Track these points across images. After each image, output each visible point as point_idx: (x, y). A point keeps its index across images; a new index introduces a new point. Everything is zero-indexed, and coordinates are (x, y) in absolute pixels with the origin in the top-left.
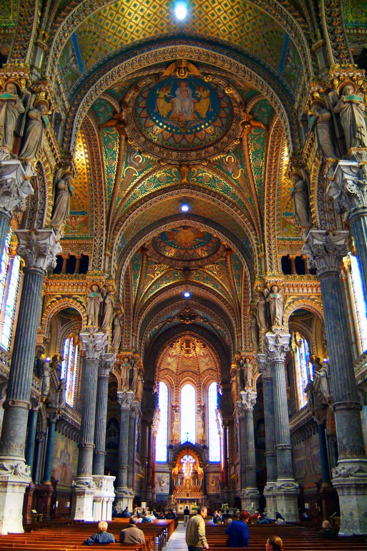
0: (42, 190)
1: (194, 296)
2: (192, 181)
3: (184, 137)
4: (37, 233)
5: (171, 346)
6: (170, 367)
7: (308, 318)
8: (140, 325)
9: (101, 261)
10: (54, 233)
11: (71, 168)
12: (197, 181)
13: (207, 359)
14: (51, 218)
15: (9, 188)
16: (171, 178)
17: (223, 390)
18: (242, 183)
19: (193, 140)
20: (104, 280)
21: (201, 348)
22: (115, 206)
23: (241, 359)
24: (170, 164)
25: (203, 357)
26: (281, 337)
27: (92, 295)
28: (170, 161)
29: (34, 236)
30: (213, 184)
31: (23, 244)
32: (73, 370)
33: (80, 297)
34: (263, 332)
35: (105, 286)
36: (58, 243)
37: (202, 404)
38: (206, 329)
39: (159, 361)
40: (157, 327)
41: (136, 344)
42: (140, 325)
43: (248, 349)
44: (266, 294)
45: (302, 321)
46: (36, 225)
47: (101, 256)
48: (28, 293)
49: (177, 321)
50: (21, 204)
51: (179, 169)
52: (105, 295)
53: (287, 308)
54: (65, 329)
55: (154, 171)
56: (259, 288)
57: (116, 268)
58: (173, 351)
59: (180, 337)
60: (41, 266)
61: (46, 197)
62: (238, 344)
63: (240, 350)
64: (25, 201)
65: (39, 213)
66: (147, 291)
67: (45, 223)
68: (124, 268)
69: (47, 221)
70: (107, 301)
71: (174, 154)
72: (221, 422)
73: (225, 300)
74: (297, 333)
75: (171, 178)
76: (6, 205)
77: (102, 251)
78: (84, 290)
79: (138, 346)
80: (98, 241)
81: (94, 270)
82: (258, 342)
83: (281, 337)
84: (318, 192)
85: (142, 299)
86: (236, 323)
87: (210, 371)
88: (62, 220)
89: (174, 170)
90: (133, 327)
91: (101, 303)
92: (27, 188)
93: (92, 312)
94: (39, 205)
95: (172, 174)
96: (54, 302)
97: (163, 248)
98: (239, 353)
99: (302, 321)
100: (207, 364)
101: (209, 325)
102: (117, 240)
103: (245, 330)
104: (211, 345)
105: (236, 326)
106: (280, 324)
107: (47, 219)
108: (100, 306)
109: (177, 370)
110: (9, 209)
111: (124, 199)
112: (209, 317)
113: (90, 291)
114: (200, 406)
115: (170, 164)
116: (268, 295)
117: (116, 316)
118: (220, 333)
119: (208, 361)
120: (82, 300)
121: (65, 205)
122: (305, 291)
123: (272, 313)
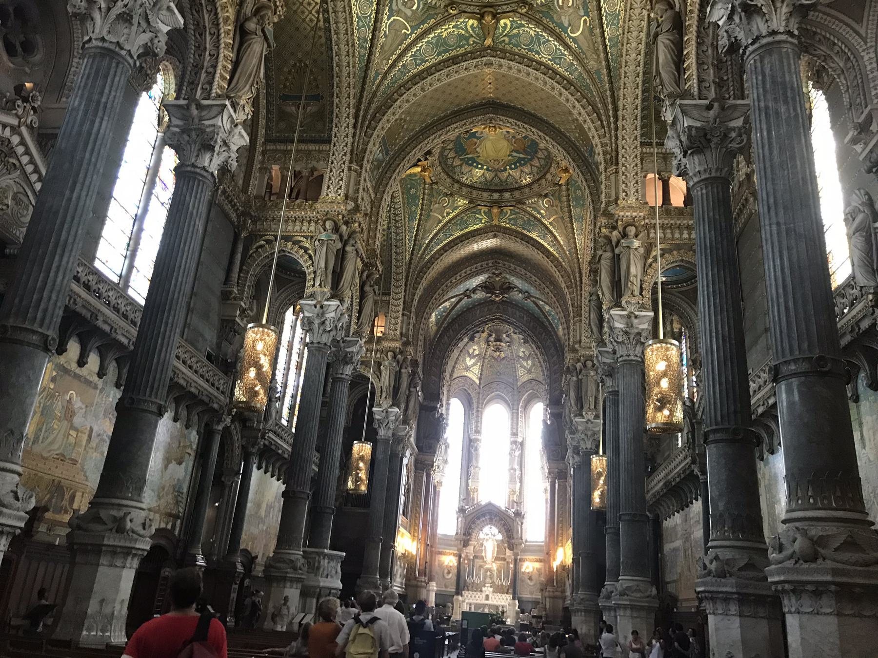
0: (213, 31)
2: (501, 43)
4: (199, 107)
5: (472, 339)
6: (469, 375)
8: (417, 298)
10: (229, 106)
12: (509, 44)
13: (530, 362)
15: (126, 6)
17: (552, 414)
18: (585, 45)
20: (344, 212)
21: (520, 345)
22: (370, 88)
24: (465, 12)
25: (523, 358)
26: (636, 317)
27: (323, 237)
29: (195, 112)
30: (536, 47)
31: (177, 126)
32: (301, 369)
33: (303, 239)
35: (346, 223)
36: (240, 127)
37: (520, 440)
38: (527, 311)
39: (451, 363)
40: (447, 304)
41: (408, 330)
42: (417, 298)
44: (614, 240)
45: (679, 292)
49: (480, 295)
50: (156, 41)
52: (346, 237)
53: (650, 265)
54: (283, 296)
56: (603, 230)
57: (373, 196)
58: (475, 347)
59: (485, 323)
63: (577, 346)
64: (163, 39)
65: (206, 72)
67: (215, 90)
68: (387, 198)
69: (220, 87)
70: (349, 248)
72: (547, 470)
73: (557, 259)
74: (675, 318)
76: (122, 40)
78: (312, 228)
79: (411, 333)
82: (601, 327)
83: (636, 317)
84: (698, 27)
85: (423, 254)
87: (534, 382)
88: (248, 87)
89: (471, 22)
90: (404, 302)
91: (338, 251)
92: (168, 14)
93: (322, 264)
94: (207, 58)
95: (467, 31)
96: (262, 246)
97: (457, 169)
98: (574, 350)
99: (679, 292)
100: (529, 371)
101: (532, 305)
102: (374, 150)
104: (535, 338)
106: (637, 293)
107: (219, 84)
108: (337, 256)
109: (480, 379)
110: (127, 47)
112: (533, 291)
113: (322, 230)
114: (515, 442)
115: (465, 12)
116: (618, 242)
117: (368, 277)
118: (550, 318)
119: (532, 367)
120: (308, 245)
121: (255, 61)
122: (685, 235)
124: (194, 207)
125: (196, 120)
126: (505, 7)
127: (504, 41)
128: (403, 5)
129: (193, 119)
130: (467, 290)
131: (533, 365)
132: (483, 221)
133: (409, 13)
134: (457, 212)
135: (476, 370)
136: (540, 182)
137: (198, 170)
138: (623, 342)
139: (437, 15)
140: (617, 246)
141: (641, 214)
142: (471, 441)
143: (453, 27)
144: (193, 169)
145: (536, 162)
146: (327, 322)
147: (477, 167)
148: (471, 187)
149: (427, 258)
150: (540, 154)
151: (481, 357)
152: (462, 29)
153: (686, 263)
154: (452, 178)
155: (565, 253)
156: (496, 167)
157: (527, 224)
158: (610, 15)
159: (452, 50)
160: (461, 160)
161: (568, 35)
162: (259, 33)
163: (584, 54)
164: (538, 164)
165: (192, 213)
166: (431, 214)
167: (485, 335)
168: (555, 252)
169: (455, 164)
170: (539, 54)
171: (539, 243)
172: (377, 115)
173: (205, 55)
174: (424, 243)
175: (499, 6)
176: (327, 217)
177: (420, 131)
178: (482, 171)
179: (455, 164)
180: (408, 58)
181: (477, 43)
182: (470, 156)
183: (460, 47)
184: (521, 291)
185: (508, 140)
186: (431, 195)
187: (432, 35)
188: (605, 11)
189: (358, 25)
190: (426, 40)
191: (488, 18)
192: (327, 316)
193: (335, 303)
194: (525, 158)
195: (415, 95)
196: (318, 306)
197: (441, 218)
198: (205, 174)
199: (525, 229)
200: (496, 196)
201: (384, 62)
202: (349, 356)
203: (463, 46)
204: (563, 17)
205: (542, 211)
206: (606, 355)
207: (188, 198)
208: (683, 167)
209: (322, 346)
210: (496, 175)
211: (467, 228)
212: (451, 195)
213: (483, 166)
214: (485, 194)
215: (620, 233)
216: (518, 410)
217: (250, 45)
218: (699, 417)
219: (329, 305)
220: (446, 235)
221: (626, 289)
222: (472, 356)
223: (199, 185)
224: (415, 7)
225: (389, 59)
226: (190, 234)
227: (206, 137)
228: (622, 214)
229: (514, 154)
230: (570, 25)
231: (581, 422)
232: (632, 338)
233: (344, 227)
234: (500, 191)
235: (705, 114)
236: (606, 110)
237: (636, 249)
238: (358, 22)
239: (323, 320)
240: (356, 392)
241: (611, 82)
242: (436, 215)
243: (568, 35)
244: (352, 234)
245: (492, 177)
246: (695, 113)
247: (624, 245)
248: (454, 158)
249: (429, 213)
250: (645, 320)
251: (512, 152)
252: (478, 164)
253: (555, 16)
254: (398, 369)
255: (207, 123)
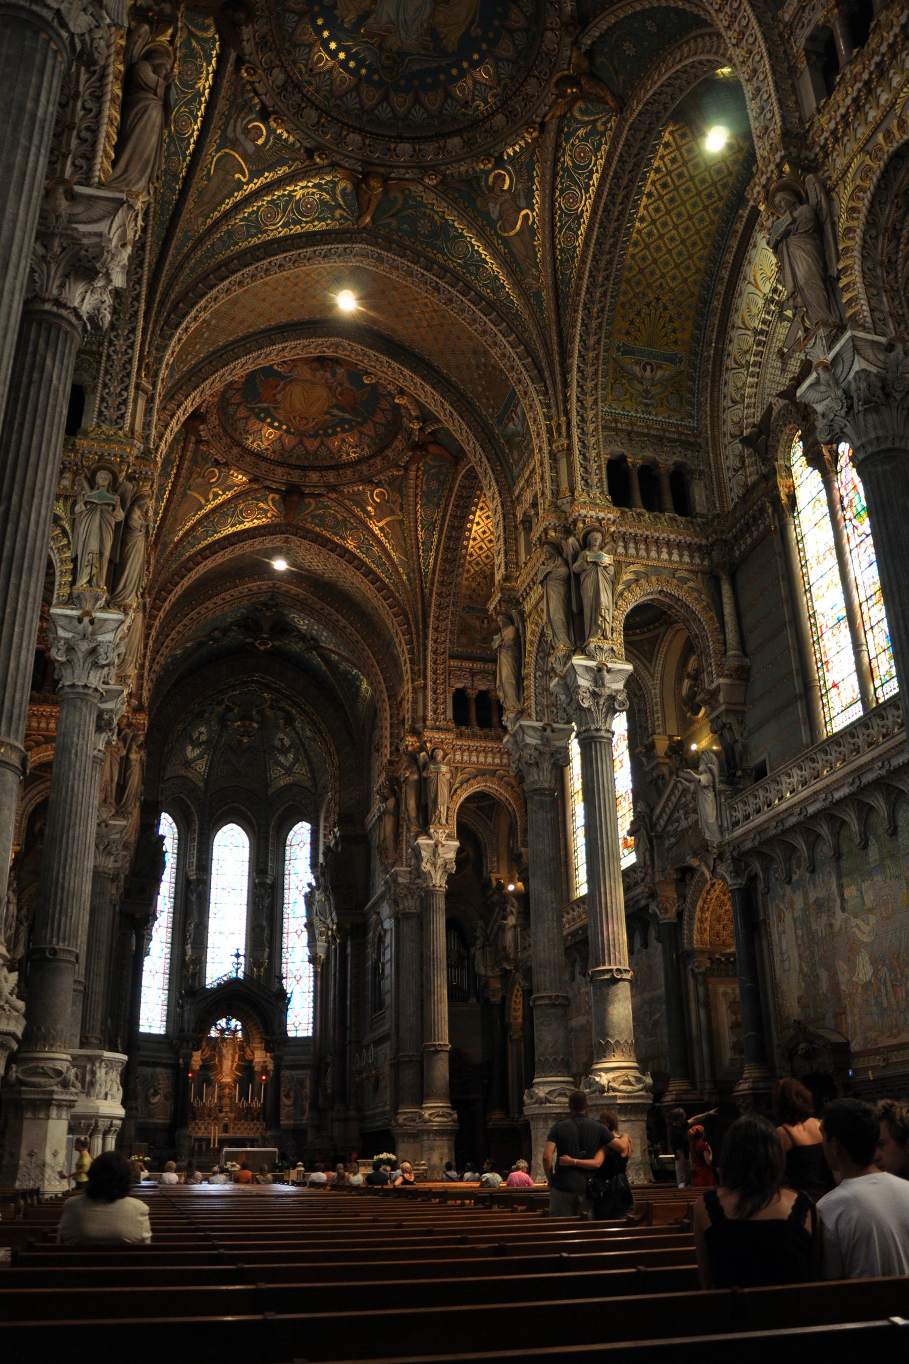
1: (298, 575)
3: (385, 98)
4: (72, 197)
7: (647, 635)
9: (125, 402)
11: (173, 36)
14: (114, 164)
16: (332, 209)
19: (409, 111)
23: (422, 748)
26: (609, 671)
28: (337, 158)
29: (63, 204)
34: (560, 654)
35: (130, 478)
43: (442, 724)
44: (569, 550)
46: (68, 170)
47: (126, 389)
48: (30, 383)
51: (357, 186)
53: (621, 594)
55: (290, 179)
58: (203, 729)
60: (76, 304)
61: (103, 94)
62: (415, 711)
63: (419, 725)
65: (78, 137)
66: (181, 540)
69: (102, 169)
71: (354, 138)
75: (332, 209)
77: (129, 375)
80: (120, 344)
81: (104, 427)
86: (411, 651)
88: (142, 183)
91: (118, 524)
93: (94, 545)
97: (241, 424)
103: (435, 672)
105: (412, 661)
107: (102, 164)
108: (116, 532)
109: (207, 782)
111: (200, 240)
119: (293, 764)
123: (587, 602)
124: (59, 379)
125: (64, 219)
126: (402, 171)
127: (390, 224)
128: (243, 133)
129: (58, 217)
130: (216, 629)
131: (296, 760)
132: (269, 515)
133: (250, 148)
134: (229, 494)
135: (201, 766)
136: (371, 462)
137: (64, 312)
138: (589, 709)
139: (294, 160)
140: (574, 560)
141: (611, 516)
142: (188, 882)
143: (313, 187)
144: (55, 309)
145: (369, 429)
146: (101, 650)
147: (271, 425)
148: (259, 456)
149: (174, 566)
150: (380, 418)
151: (210, 745)
152: (327, 193)
153: (666, 596)
154: (231, 437)
155: (401, 578)
156: (302, 429)
157: (340, 526)
158: (567, 215)
159: (307, 222)
160: (252, 410)
161: (496, 233)
162: (161, 91)
163: (518, 265)
164: (372, 433)
165: (57, 391)
166: (189, 492)
167: (220, 709)
168: (383, 576)
169: (238, 415)
170: (444, 254)
171: (359, 559)
172: (181, 305)
173: (75, 105)
174: (172, 541)
175: (395, 167)
176: (103, 464)
177: (224, 347)
178: (278, 433)
179: (238, 415)
180: (238, 220)
181: (346, 219)
182: (265, 405)
183: (320, 220)
184: (302, 637)
185: (330, 389)
186: (194, 461)
187: (280, 193)
188: (560, 208)
189: (168, 149)
190: (269, 198)
191: (376, 185)
192: (100, 638)
193: (113, 615)
194: (351, 420)
195: (241, 284)
196: (86, 620)
197: (203, 502)
198: (73, 319)
199: (336, 534)
200: (296, 477)
201: (201, 220)
202: (106, 717)
203: (324, 219)
204: (491, 205)
205: (369, 508)
206: (531, 732)
207: (49, 362)
208: (838, 430)
209: (90, 691)
210: (301, 442)
211: (243, 522)
212: (226, 464)
213: (281, 424)
214: (280, 471)
215: (578, 540)
216: (268, 833)
217: (146, 109)
218: (659, 829)
219: (106, 620)
220: (207, 531)
221: (594, 628)
222: (196, 744)
223: (65, 341)
224: (260, 142)
225: (208, 217)
226: (55, 428)
227: (83, 253)
228: (583, 512)
229: (336, 412)
230: (500, 217)
231: (428, 845)
232: (601, 703)
233: (130, 486)
234: (305, 468)
235: (882, 358)
236: (549, 354)
237: (605, 568)
238: (169, 145)
239: (94, 644)
240: (34, 792)
241: (558, 315)
242: (196, 495)
243: (496, 232)
244: (137, 499)
245: (292, 444)
246: (869, 353)
247: (589, 560)
248: (239, 405)
249: (185, 491)
250: (619, 677)
251: (332, 407)
252: (274, 420)
253: (479, 202)
254: (124, 753)
255: (82, 228)
